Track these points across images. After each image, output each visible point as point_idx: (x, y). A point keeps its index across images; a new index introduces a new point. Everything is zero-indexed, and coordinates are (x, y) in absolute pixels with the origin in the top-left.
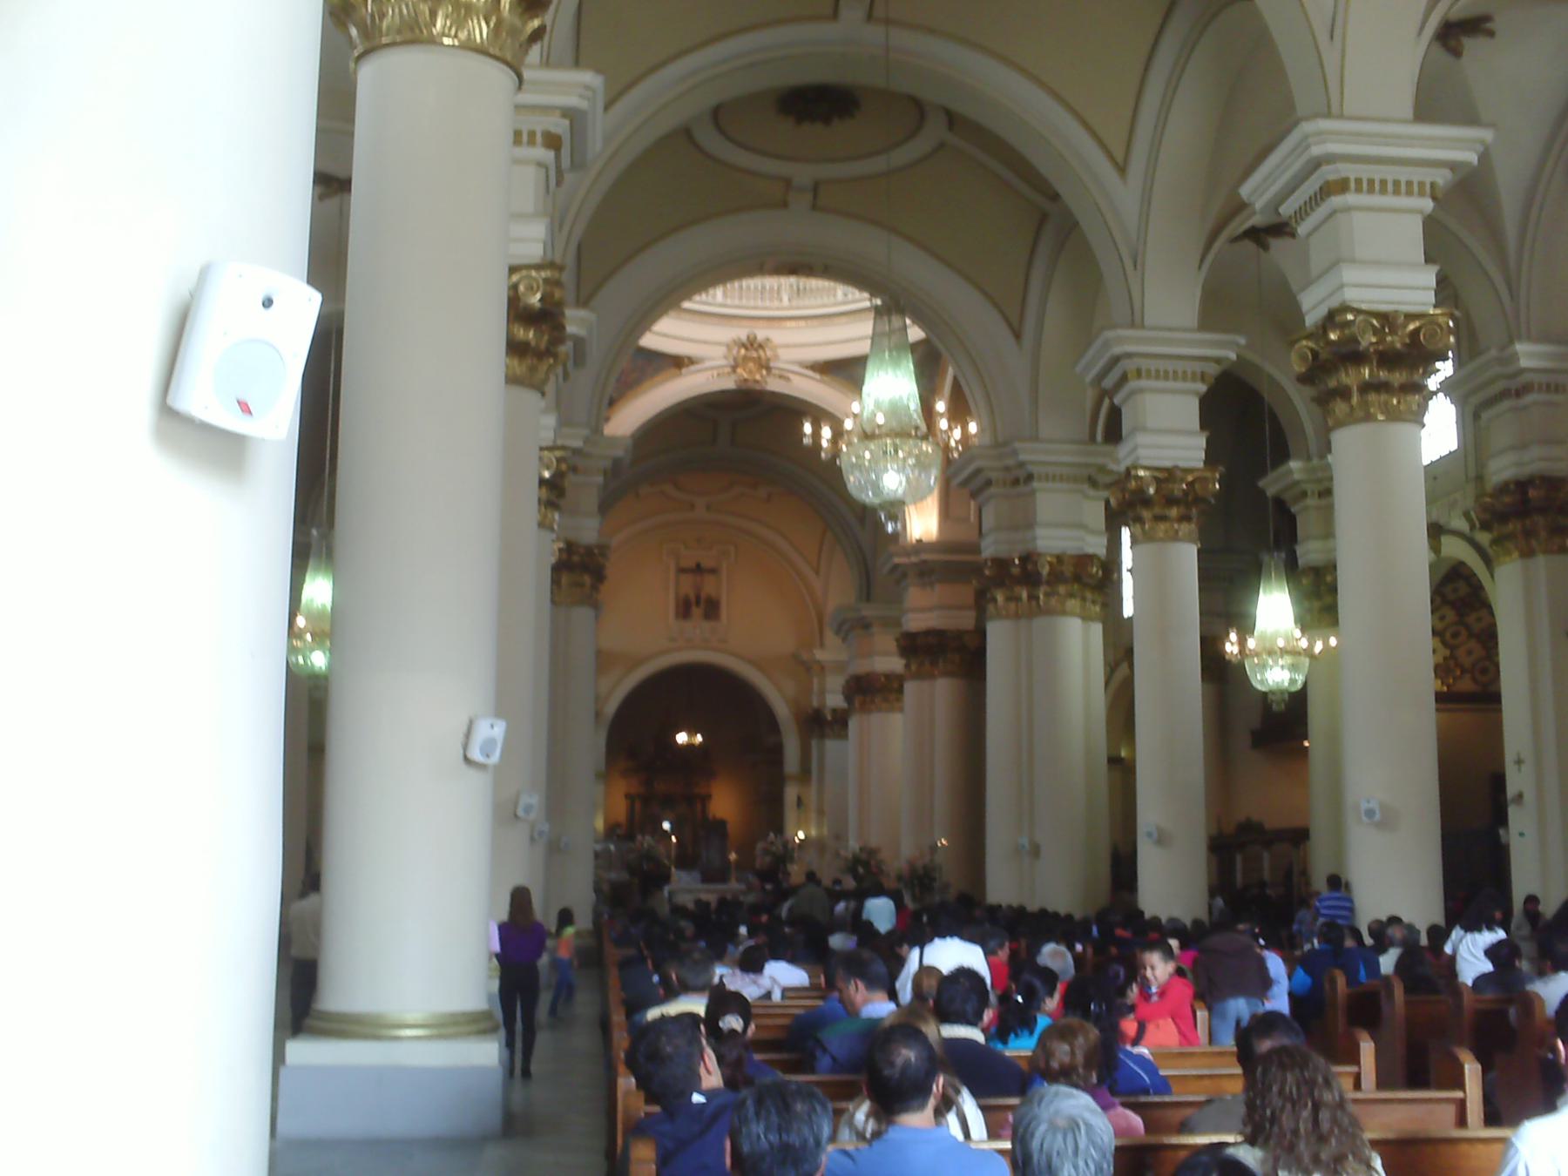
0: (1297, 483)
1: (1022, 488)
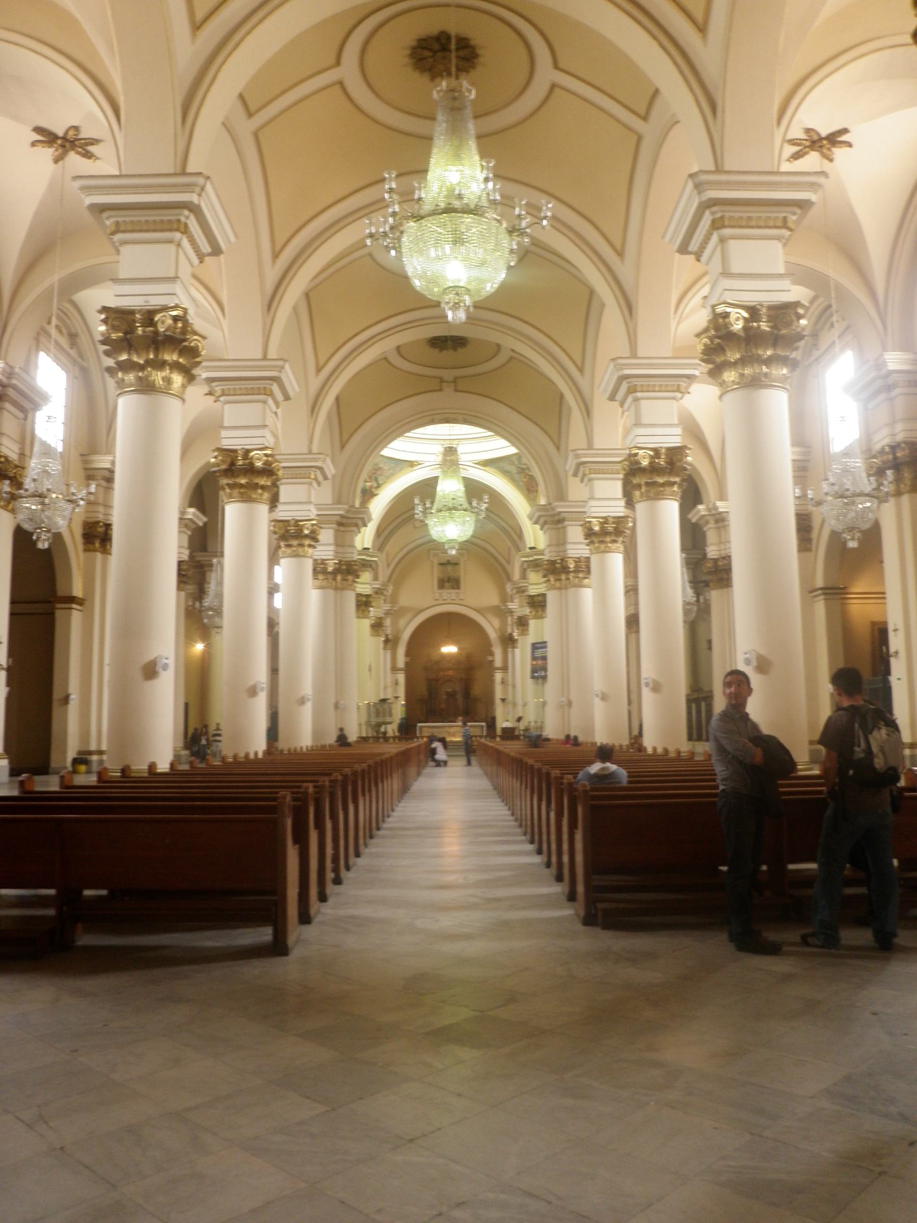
0: (704, 516)
1: (560, 525)
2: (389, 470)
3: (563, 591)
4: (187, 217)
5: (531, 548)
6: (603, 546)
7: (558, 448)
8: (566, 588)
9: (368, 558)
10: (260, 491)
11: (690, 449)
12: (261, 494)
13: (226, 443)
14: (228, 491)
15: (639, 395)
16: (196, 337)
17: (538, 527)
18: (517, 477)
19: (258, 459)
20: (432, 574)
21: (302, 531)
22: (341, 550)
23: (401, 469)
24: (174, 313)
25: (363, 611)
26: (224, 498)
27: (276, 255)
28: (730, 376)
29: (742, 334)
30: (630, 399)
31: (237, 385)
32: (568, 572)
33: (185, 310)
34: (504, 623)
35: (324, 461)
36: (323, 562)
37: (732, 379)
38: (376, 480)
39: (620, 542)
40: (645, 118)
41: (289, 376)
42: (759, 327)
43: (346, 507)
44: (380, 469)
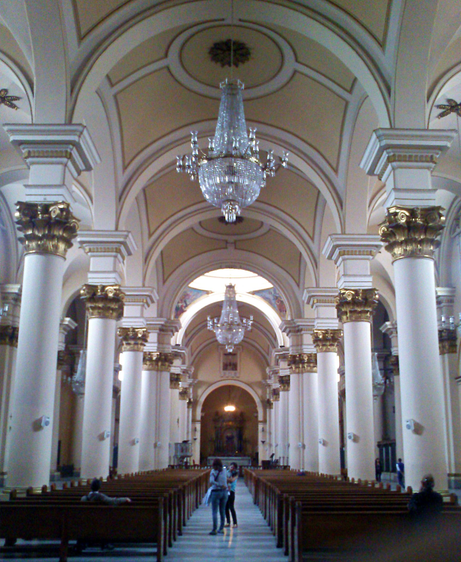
0: (390, 329)
1: (299, 334)
2: (194, 295)
3: (300, 375)
4: (71, 149)
5: (281, 347)
6: (324, 348)
7: (298, 285)
8: (302, 373)
9: (179, 351)
10: (111, 312)
11: (377, 290)
12: (112, 314)
13: (91, 282)
14: (91, 311)
15: (346, 257)
16: (74, 220)
17: (285, 334)
18: (273, 302)
19: (111, 292)
20: (220, 361)
21: (137, 335)
22: (161, 346)
23: (201, 295)
24: (61, 206)
25: (175, 384)
26: (89, 315)
27: (125, 168)
28: (398, 250)
29: (406, 225)
30: (340, 259)
31: (99, 246)
32: (303, 363)
33: (68, 205)
34: (264, 393)
35: (152, 292)
36: (150, 353)
37: (399, 253)
38: (185, 302)
39: (335, 345)
40: (350, 92)
41: (132, 242)
42: (416, 221)
43: (165, 319)
44: (188, 295)
